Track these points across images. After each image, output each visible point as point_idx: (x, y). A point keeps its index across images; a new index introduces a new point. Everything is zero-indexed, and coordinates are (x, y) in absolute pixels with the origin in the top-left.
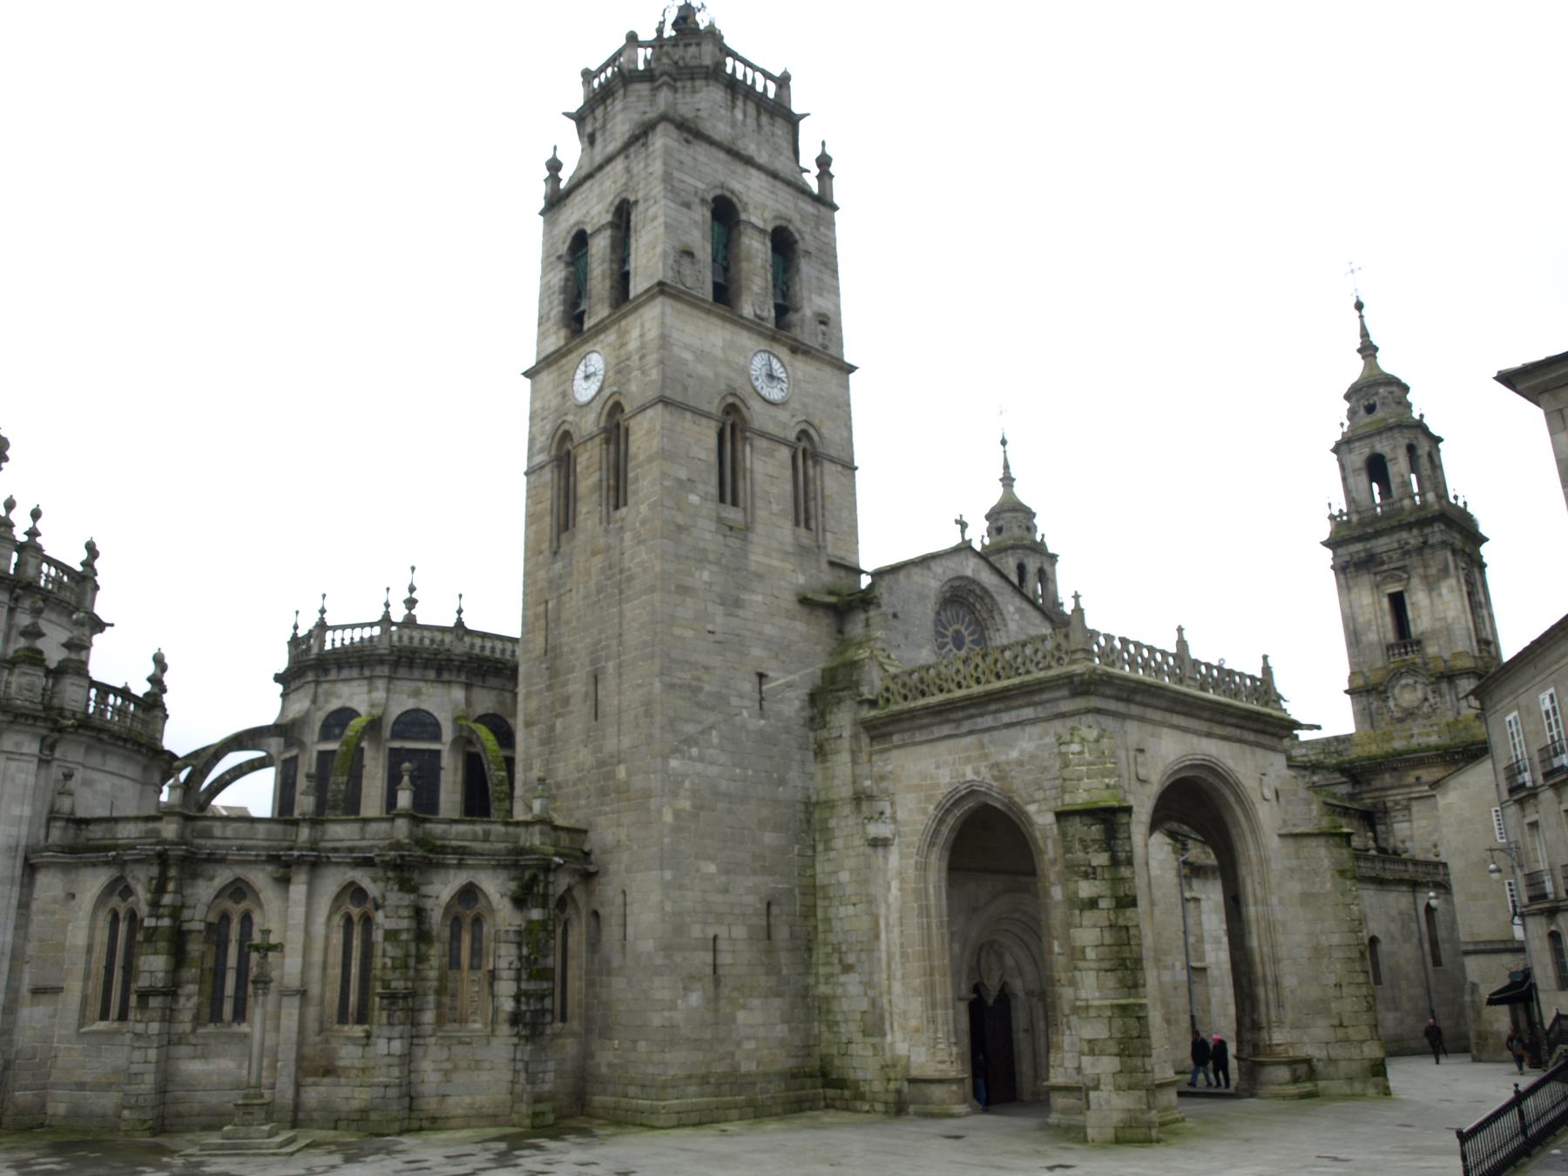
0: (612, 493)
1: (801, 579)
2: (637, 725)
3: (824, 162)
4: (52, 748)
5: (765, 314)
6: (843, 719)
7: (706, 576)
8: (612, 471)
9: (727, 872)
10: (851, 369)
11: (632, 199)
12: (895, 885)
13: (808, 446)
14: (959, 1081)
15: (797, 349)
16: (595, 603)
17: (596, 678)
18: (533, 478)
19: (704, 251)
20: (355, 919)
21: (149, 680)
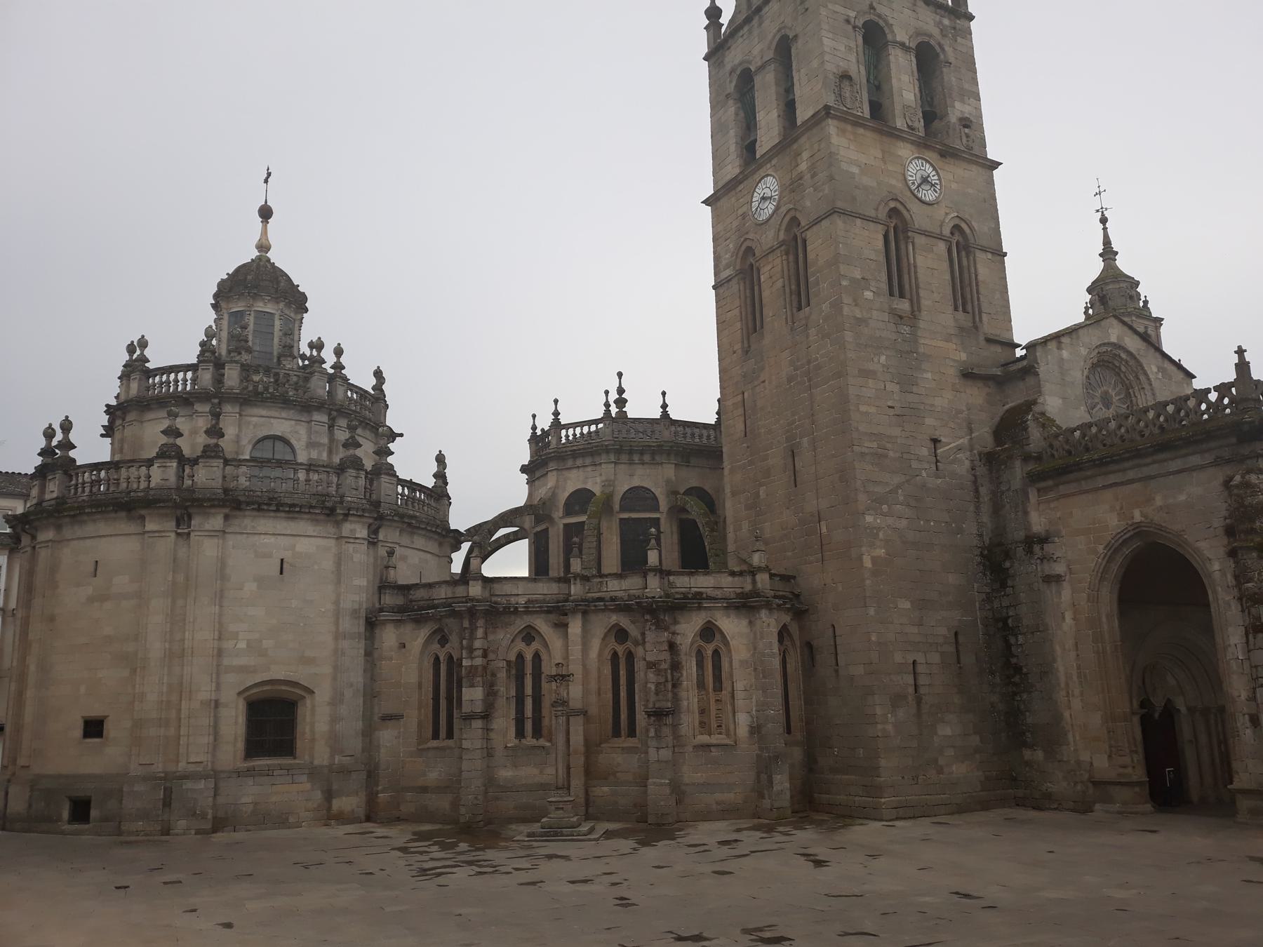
1: (963, 356)
4: (376, 532)
5: (916, 125)
7: (883, 358)
10: (996, 165)
12: (1068, 616)
13: (961, 240)
14: (1139, 783)
15: (948, 154)
19: (859, 72)
20: (620, 654)
21: (435, 476)
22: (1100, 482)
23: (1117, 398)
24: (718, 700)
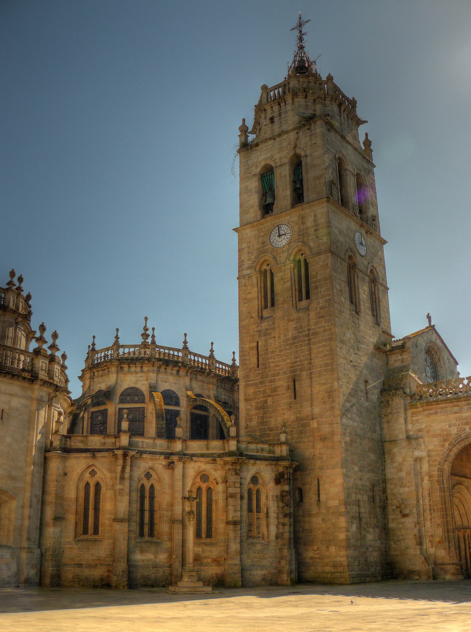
0: (297, 292)
3: (368, 143)
9: (361, 471)
10: (385, 242)
11: (303, 154)
17: (294, 380)
23: (432, 370)
24: (257, 518)
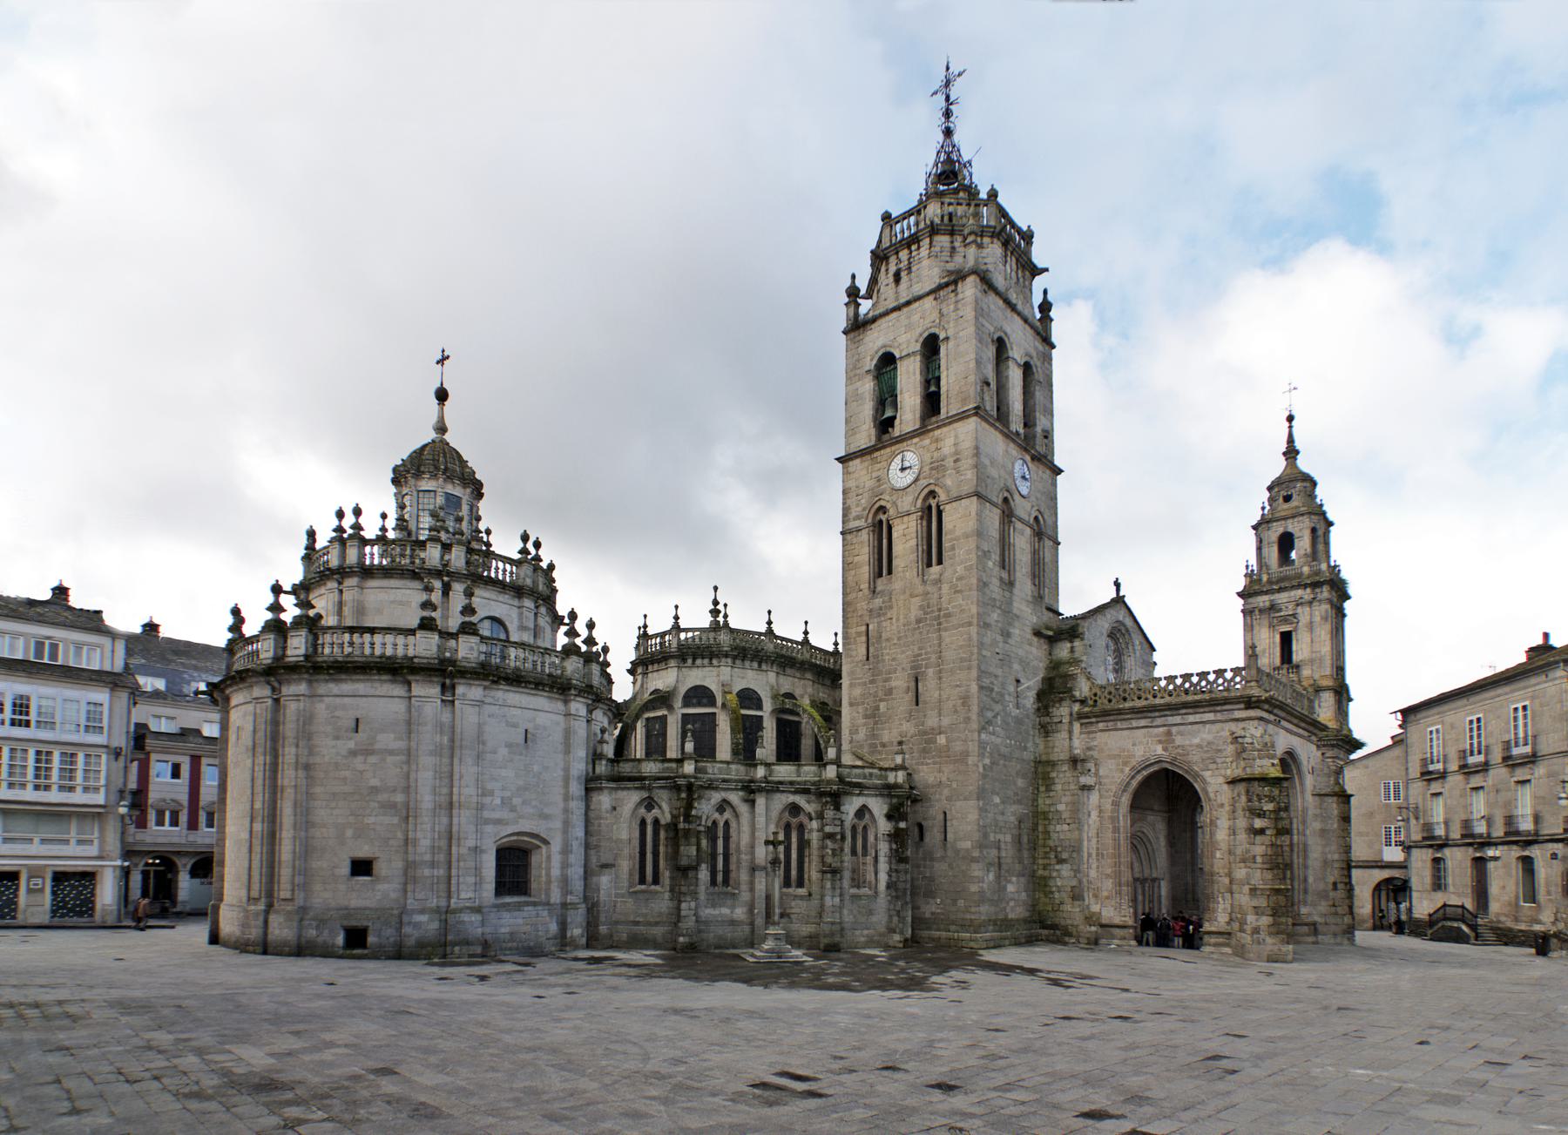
2: (956, 711)
6: (1063, 711)
8: (925, 540)
16: (915, 629)
18: (849, 537)
22: (1135, 723)
